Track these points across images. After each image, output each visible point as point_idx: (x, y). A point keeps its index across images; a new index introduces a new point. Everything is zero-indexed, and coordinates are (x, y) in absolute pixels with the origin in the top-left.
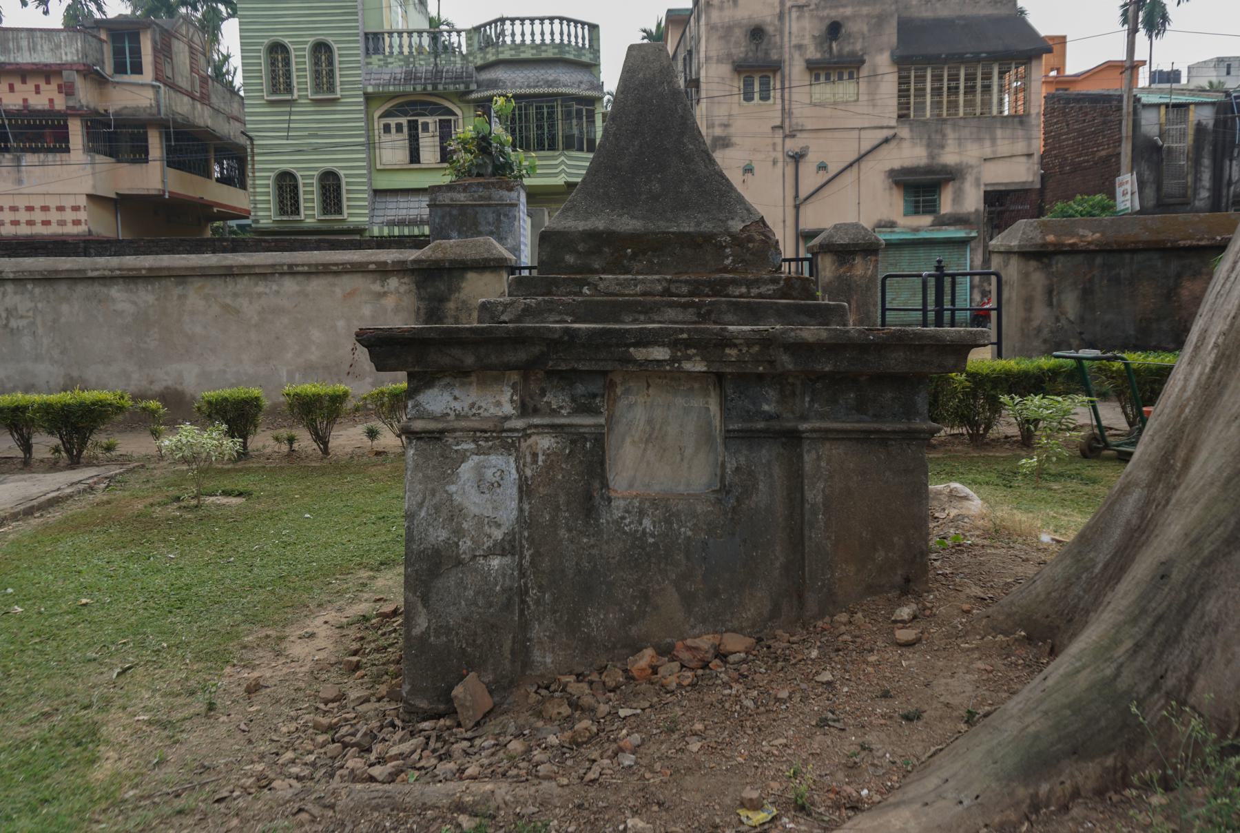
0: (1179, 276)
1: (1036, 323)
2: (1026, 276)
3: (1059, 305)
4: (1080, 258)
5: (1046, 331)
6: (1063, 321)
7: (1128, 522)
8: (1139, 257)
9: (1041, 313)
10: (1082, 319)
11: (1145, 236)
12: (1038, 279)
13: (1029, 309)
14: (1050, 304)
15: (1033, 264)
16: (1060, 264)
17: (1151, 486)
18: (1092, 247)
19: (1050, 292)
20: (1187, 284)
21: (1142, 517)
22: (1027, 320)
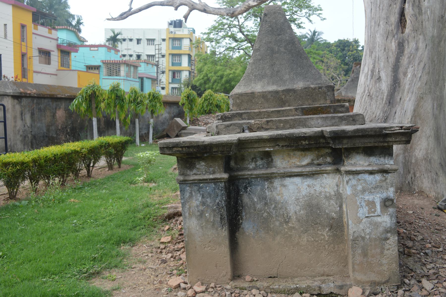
0: (56, 109)
1: (18, 128)
2: (14, 106)
3: (25, 120)
4: (30, 100)
5: (21, 131)
6: (26, 127)
7: (402, 162)
8: (46, 101)
9: (19, 123)
10: (31, 125)
11: (48, 93)
12: (18, 107)
13: (15, 122)
14: (22, 120)
15: (16, 101)
16: (25, 101)
17: (404, 153)
18: (35, 95)
19: (22, 114)
20: (57, 112)
21: (406, 160)
22: (15, 127)
